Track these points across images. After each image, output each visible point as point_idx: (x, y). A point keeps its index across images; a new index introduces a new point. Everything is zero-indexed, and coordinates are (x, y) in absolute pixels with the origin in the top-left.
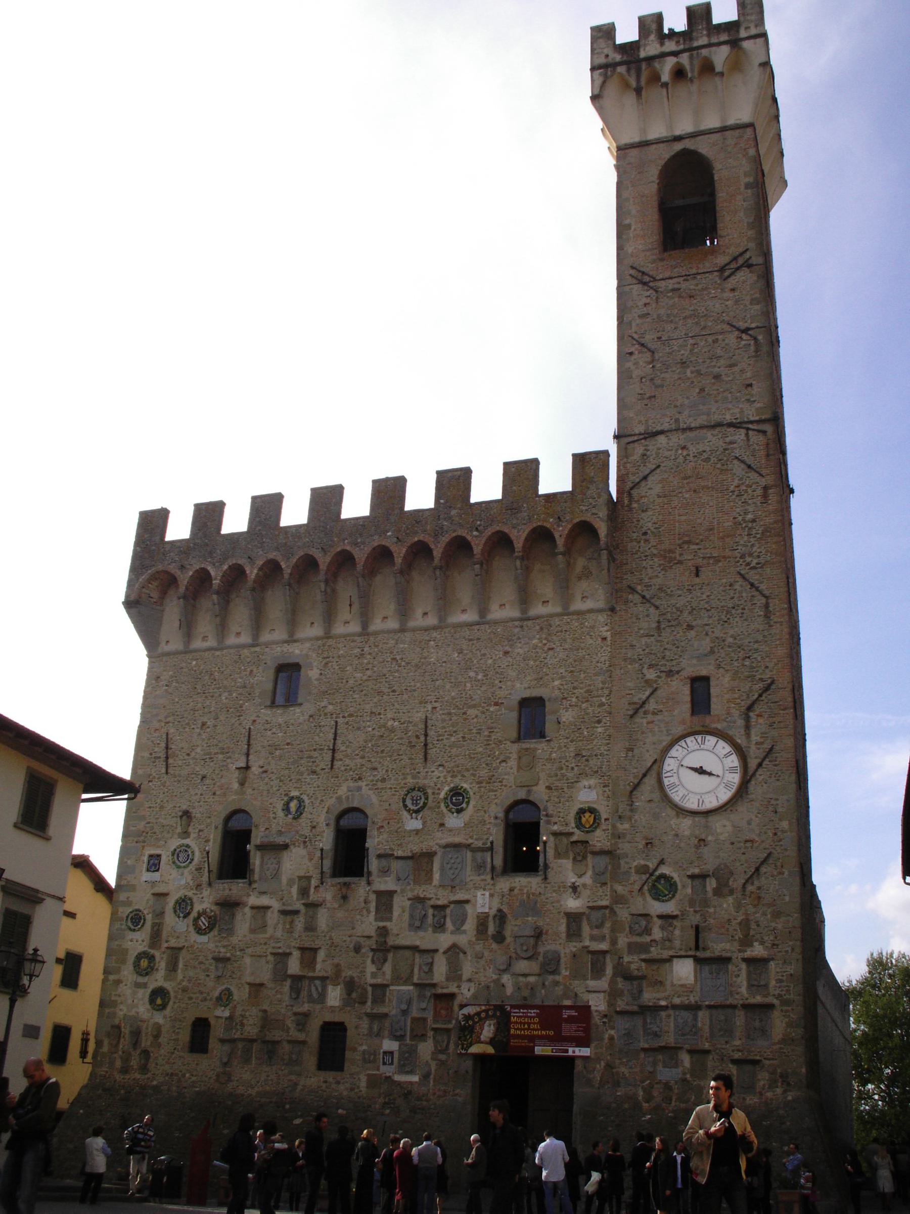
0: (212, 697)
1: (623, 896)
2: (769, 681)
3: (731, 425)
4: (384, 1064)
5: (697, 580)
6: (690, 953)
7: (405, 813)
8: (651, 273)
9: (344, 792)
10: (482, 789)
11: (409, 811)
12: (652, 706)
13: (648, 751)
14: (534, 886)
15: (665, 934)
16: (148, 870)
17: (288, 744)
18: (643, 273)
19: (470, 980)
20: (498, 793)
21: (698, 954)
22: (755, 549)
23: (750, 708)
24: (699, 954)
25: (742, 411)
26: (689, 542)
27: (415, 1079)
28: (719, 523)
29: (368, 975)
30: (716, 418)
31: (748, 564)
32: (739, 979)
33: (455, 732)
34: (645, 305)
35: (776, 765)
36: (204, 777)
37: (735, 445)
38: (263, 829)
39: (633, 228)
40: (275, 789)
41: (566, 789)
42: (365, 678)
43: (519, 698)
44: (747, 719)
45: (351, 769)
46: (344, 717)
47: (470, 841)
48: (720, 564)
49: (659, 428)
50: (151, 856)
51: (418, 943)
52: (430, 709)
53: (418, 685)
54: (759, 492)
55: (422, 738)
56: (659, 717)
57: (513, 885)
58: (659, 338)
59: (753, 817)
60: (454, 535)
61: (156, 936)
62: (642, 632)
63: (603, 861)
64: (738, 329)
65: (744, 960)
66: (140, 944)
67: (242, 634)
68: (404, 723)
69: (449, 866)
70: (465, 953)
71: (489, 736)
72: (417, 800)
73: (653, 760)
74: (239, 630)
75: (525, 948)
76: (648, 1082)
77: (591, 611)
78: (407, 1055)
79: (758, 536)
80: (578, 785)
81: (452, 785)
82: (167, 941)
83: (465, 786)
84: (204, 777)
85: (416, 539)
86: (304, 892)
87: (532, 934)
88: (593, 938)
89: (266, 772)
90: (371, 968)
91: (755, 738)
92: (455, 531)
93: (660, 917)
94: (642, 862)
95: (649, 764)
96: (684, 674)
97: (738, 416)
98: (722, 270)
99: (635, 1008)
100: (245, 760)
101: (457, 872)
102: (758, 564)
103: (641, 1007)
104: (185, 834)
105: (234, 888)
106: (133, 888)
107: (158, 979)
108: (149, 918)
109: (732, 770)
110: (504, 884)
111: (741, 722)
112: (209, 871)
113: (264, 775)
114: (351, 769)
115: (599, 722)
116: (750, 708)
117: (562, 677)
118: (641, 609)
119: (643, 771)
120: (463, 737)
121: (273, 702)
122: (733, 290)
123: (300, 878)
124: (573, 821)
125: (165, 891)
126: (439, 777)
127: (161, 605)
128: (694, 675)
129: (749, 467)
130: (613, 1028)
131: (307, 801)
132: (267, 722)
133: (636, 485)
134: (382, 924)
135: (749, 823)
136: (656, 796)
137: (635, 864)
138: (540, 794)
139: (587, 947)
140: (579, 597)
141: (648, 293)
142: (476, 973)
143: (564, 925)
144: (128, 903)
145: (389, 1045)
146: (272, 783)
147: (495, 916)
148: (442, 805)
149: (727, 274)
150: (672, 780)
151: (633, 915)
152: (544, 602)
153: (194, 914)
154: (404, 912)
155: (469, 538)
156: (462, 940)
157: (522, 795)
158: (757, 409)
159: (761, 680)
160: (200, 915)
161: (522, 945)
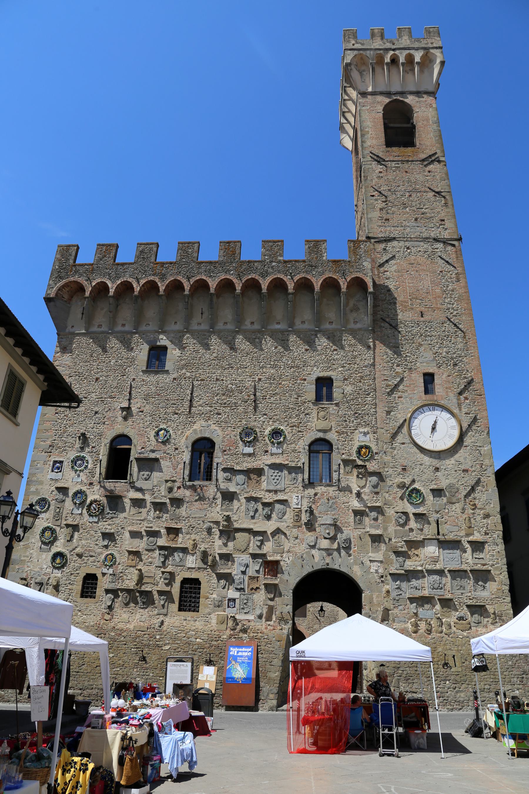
0: (104, 362)
2: (470, 379)
3: (434, 239)
4: (228, 607)
5: (422, 319)
6: (434, 537)
7: (241, 443)
8: (382, 157)
9: (199, 428)
10: (294, 431)
11: (243, 441)
12: (401, 387)
13: (400, 413)
14: (331, 492)
15: (418, 525)
16: (53, 471)
17: (159, 395)
18: (378, 156)
19: (289, 551)
20: (304, 433)
21: (440, 537)
22: (454, 306)
23: (460, 393)
24: (441, 537)
25: (440, 232)
26: (416, 298)
27: (251, 617)
28: (432, 290)
29: (217, 548)
30: (425, 235)
31: (452, 313)
32: (466, 555)
33: (274, 394)
34: (380, 172)
35: (478, 427)
36: (96, 413)
37: (438, 250)
38: (140, 448)
39: (370, 133)
40: (148, 423)
41: (349, 434)
42: (212, 358)
43: (316, 377)
44: (459, 399)
45: (203, 413)
46: (197, 380)
47: (286, 462)
48: (436, 312)
49: (392, 235)
50: (55, 462)
51: (251, 526)
52: (257, 379)
53: (249, 364)
54: (454, 275)
55: (252, 397)
56: (406, 394)
57: (316, 491)
58: (389, 190)
59: (468, 456)
60: (275, 277)
61: (58, 516)
62: (391, 345)
63: (374, 479)
64: (434, 191)
65: (468, 542)
66: (45, 521)
67: (126, 325)
68: (240, 387)
69: (273, 477)
70: (285, 534)
71: (297, 399)
72: (249, 435)
73: (404, 419)
74: (124, 322)
75: (327, 531)
76: (413, 620)
77: (360, 329)
78: (245, 601)
79: (456, 299)
80: (357, 431)
81: (273, 427)
82: (66, 520)
83: (282, 428)
84: (96, 413)
85: (250, 277)
86: (170, 490)
87: (332, 522)
88: (371, 526)
89: (142, 412)
90: (218, 543)
91: (464, 410)
92: (275, 274)
93: (414, 514)
95: (401, 422)
96: (419, 370)
97: (438, 235)
98: (423, 160)
99: (403, 572)
100: (128, 404)
101: (278, 482)
102: (457, 314)
103: (406, 571)
104: (82, 449)
105: (118, 486)
106: (41, 483)
107: (59, 547)
108: (53, 503)
109: (452, 427)
110: (311, 491)
111: (455, 401)
112: (100, 474)
113: (141, 413)
114: (203, 413)
115: (368, 394)
116: (460, 393)
117: (343, 367)
118: (389, 332)
119: (398, 424)
120: (280, 398)
121: (147, 368)
122: (429, 172)
123: (167, 481)
124: (355, 453)
125: (66, 486)
126: (264, 422)
127: (69, 303)
128: (425, 371)
129: (447, 262)
130: (388, 584)
131: (171, 432)
132: (143, 380)
133: (381, 265)
134: (227, 514)
135: (465, 458)
136: (407, 440)
137: (396, 481)
138: (332, 436)
139: (368, 532)
140: (352, 321)
141: (381, 167)
142: (294, 547)
143: (353, 517)
144: (37, 492)
145: (232, 594)
146: (146, 419)
147: (306, 511)
148: (266, 438)
149: (425, 163)
150: (416, 431)
151: (397, 513)
152: (330, 322)
153: (88, 502)
154: (241, 506)
155: (285, 279)
156: (283, 526)
157: (320, 435)
158: (449, 233)
159: (465, 378)
160: (91, 503)
161: (325, 529)
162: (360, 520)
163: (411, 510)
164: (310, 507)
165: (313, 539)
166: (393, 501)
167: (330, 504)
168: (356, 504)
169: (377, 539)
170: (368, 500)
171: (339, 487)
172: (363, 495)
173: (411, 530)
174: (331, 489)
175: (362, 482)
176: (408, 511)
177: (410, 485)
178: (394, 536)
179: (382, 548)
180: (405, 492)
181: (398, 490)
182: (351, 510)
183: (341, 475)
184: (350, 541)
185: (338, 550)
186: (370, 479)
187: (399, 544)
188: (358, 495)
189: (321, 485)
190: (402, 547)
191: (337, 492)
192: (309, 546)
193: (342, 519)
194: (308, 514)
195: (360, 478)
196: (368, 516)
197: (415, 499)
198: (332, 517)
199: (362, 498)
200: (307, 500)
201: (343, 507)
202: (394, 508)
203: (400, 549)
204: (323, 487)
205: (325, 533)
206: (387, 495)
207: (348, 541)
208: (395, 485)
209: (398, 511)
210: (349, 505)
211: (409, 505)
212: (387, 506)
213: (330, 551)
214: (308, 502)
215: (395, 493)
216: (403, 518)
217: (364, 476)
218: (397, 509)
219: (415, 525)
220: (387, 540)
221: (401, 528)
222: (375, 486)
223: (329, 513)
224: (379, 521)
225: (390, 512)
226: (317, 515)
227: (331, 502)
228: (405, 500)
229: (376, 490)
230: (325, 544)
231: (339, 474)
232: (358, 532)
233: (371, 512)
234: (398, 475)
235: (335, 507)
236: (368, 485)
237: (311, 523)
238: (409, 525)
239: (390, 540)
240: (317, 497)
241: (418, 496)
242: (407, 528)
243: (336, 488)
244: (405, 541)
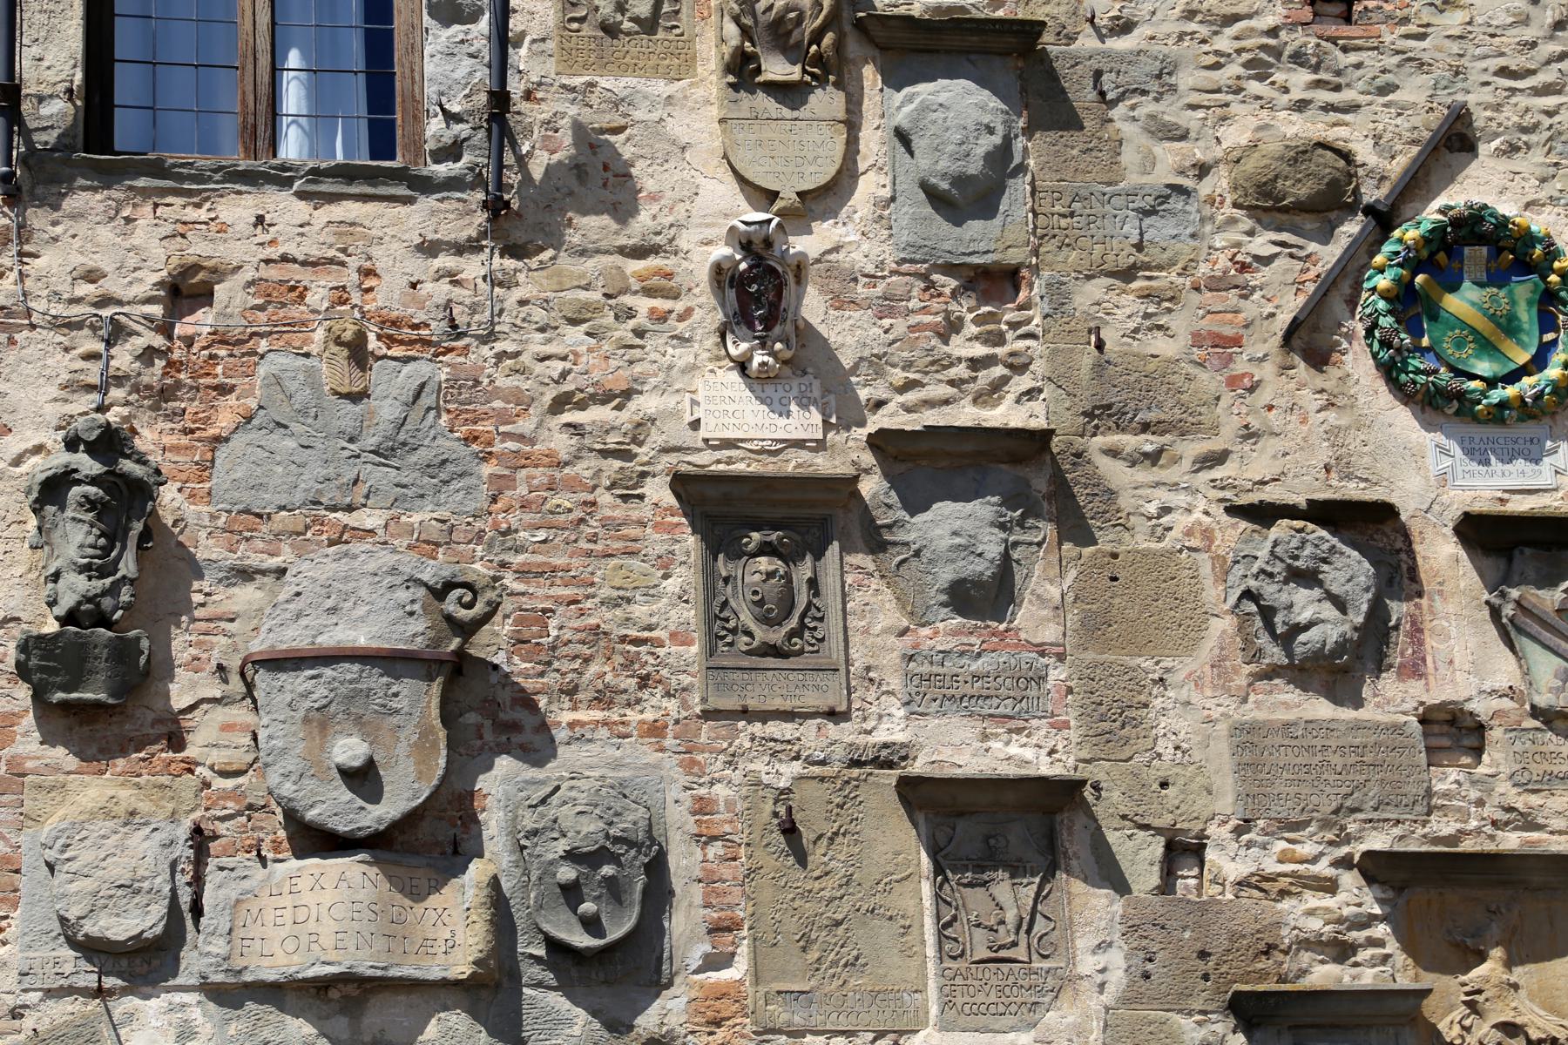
1: (1156, 377)
14: (397, 266)
15: (1545, 666)
57: (198, 248)
63: (959, 108)
75: (349, 749)
87: (412, 633)
88: (931, 689)
93: (1488, 535)
94: (1299, 128)
137: (1235, 135)
139: (887, 757)
143: (684, 578)
151: (1263, 515)
161: (321, 721)
162: (777, 607)
163: (1432, 477)
164: (110, 443)
165: (147, 853)
166: (1209, 382)
167: (386, 410)
168: (728, 413)
169: (1005, 832)
170: (876, 364)
171: (496, 207)
172: (813, 306)
173: (1453, 731)
174: (393, 229)
175: (800, 148)
176: (1407, 492)
177: (1418, 183)
178: (1226, 803)
179: (1087, 964)
180: (1344, 281)
181: (1262, 243)
182: (658, 492)
183: (520, 57)
184: (657, 868)
185: (490, 991)
186: (885, 104)
187: (1305, 914)
188: (758, 290)
189: (252, 179)
190: (1342, 951)
191: (473, 267)
192: (92, 949)
193: (541, 593)
194: (76, 536)
195: (774, 88)
196: (875, 540)
197: (1487, 346)
198: (409, 563)
199: (805, 335)
200: (63, 365)
201: (562, 444)
202: (1219, 458)
203: (1323, 975)
204: (286, 208)
205: (313, 767)
206: (1127, 306)
207: (630, 867)
208: (1219, 182)
209: (1272, 494)
210: (642, 426)
211: (1403, 419)
212: (1130, 442)
213: (379, 1016)
214: (76, 386)
215: (1217, 284)
216: (1334, 577)
217: (828, 69)
218: (1252, 471)
219: (1503, 669)
220: (1141, 858)
221: (1321, 709)
222: (964, 199)
223: (369, 519)
224: (1033, 619)
225: (1169, 507)
226: (207, 549)
227: (392, 383)
228: (1357, 364)
229: (979, 239)
230: (313, 915)
231: (503, 40)
232: (757, 767)
233: (915, 505)
234: (1259, 69)
235: (449, 445)
236: (870, 187)
237: (124, 652)
238: (1415, 669)
239: (1182, 851)
240: (200, 323)
241: (1527, 316)
242: (1392, 700)
243: (459, 217)
244: (1375, 868)
